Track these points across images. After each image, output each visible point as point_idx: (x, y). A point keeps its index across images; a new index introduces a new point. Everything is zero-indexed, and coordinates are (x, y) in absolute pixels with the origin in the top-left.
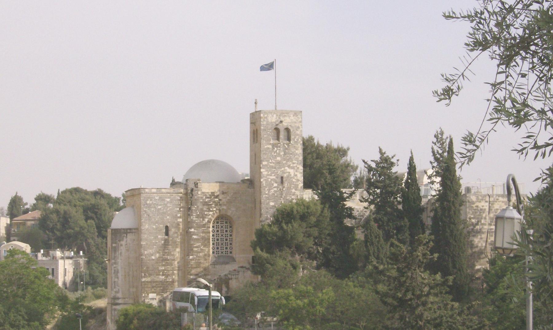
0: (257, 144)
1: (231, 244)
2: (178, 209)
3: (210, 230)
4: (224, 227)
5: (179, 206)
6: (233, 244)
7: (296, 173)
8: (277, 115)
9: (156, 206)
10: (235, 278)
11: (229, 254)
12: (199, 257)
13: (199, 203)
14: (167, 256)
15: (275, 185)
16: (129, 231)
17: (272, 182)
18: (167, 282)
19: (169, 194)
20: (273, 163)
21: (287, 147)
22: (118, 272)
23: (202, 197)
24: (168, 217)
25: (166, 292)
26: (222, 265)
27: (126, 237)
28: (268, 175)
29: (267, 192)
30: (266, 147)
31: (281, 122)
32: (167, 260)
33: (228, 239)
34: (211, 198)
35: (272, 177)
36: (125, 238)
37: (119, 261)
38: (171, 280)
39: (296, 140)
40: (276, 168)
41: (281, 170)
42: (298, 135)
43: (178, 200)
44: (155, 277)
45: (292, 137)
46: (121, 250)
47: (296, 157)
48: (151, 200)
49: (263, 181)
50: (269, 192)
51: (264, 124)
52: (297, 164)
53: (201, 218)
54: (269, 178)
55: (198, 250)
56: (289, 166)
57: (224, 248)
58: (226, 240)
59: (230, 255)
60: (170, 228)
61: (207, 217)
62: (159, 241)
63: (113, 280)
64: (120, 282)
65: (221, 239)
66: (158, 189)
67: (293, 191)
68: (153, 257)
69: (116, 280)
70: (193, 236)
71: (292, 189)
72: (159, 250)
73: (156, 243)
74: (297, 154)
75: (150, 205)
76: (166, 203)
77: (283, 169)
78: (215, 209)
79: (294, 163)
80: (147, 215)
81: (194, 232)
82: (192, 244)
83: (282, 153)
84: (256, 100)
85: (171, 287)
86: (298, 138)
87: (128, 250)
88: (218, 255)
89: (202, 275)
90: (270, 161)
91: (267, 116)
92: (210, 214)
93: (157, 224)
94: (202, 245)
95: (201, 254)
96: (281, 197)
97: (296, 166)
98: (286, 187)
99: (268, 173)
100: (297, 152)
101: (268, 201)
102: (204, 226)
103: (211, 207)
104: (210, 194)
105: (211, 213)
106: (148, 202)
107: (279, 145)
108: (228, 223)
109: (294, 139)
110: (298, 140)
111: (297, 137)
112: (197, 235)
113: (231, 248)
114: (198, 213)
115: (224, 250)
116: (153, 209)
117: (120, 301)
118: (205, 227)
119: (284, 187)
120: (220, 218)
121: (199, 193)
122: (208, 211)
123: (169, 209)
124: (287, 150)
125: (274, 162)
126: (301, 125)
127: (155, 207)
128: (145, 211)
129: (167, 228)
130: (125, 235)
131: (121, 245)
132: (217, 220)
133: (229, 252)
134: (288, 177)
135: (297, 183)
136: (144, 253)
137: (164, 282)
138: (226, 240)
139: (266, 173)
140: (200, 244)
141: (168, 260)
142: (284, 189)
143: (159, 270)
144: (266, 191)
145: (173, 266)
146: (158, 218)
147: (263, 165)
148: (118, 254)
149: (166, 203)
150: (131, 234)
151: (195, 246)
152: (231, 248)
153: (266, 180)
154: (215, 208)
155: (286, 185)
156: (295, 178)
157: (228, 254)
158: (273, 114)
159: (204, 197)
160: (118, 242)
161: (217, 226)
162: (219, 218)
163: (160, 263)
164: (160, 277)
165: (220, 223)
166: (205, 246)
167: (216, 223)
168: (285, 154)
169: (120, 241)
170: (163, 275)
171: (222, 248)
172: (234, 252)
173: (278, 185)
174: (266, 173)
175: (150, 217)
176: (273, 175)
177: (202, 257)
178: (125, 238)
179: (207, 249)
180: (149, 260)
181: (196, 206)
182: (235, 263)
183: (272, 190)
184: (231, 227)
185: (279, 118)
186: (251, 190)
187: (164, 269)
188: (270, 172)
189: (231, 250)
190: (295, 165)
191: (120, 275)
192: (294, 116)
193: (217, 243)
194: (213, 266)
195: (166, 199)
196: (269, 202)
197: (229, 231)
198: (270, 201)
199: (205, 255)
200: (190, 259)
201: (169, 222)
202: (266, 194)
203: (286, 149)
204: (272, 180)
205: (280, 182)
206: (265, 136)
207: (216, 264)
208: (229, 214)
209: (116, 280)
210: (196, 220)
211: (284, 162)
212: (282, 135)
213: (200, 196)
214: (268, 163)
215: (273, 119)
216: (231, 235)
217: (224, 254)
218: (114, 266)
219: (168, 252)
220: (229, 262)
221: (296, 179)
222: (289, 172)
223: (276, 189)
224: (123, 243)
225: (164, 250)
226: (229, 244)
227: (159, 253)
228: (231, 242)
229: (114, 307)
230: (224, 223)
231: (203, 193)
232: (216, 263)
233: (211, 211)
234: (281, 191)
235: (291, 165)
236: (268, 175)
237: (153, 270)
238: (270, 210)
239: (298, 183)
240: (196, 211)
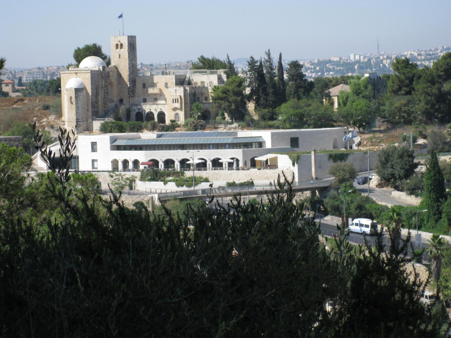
0: (122, 50)
22: (79, 107)
37: (79, 102)
64: (80, 112)
69: (78, 111)
117: (80, 120)
131: (80, 95)
148: (78, 99)
191: (80, 108)
209: (78, 111)
212: (132, 47)
224: (81, 94)
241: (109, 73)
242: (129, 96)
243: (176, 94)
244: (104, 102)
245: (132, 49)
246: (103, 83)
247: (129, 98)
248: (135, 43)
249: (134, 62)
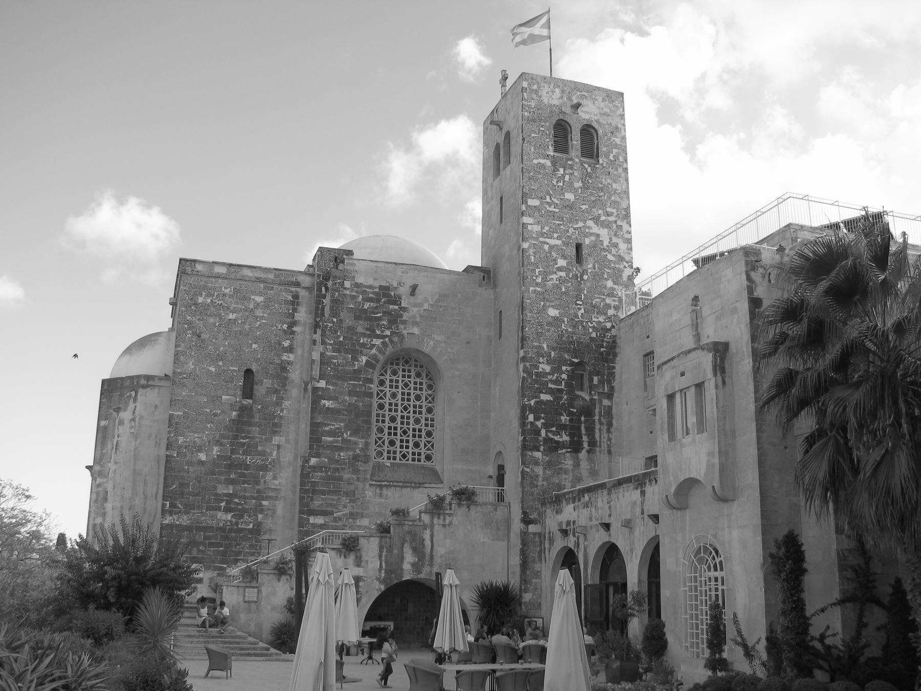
1: (429, 434)
2: (285, 327)
3: (371, 388)
4: (412, 385)
5: (289, 320)
6: (434, 434)
7: (615, 240)
8: (563, 91)
9: (222, 311)
10: (444, 526)
11: (422, 462)
12: (337, 462)
13: (345, 311)
14: (243, 454)
15: (562, 263)
16: (143, 382)
17: (554, 255)
18: (240, 531)
19: (262, 286)
20: (556, 206)
21: (589, 170)
22: (105, 499)
23: (354, 297)
24: (254, 346)
25: (236, 561)
26: (404, 490)
27: (135, 400)
28: (542, 234)
29: (539, 280)
30: (535, 161)
31: (577, 106)
32: (244, 466)
33: (423, 421)
34: (378, 301)
35: (552, 242)
36: (132, 400)
37: (111, 466)
38: (251, 526)
39: (611, 158)
40: (563, 220)
41: (575, 226)
42: (616, 146)
43: (286, 302)
44: (203, 514)
45: (604, 149)
46: (118, 436)
47: (613, 198)
48: (209, 295)
49: (530, 247)
50: (545, 279)
51: (529, 106)
52: (617, 216)
53: (347, 351)
55: (337, 441)
56: (596, 220)
57: (411, 444)
58: (417, 421)
59: (428, 463)
60: (257, 377)
61: (365, 351)
62: (223, 412)
63: (91, 519)
65: (402, 417)
66: (231, 265)
67: (610, 284)
68: (203, 457)
70: (323, 402)
71: (606, 279)
72: (222, 436)
73: (215, 415)
74: (615, 193)
75: (206, 306)
76: (251, 306)
77: (581, 224)
78: (388, 333)
79: (609, 214)
80: (194, 334)
81: (326, 388)
82: (319, 423)
83: (578, 184)
85: (252, 546)
86: (618, 154)
87: (135, 436)
88: (392, 461)
89: (344, 515)
90: (548, 200)
91: (539, 88)
92: (374, 345)
93: (221, 363)
94: (347, 427)
95: (342, 454)
96: (578, 297)
97: (616, 222)
98: (589, 271)
99: (542, 228)
100: (614, 186)
101: (542, 303)
102: (356, 375)
103: (378, 325)
104: (377, 290)
105: (377, 342)
106: (200, 300)
107: (570, 162)
108: (424, 375)
109: (607, 156)
110: (616, 157)
111: (615, 151)
112: (335, 399)
113: (429, 446)
114: (341, 339)
115: (410, 450)
116: (212, 320)
118: (359, 379)
119: (584, 272)
120: (401, 362)
121: (347, 284)
122: (369, 336)
123: (258, 323)
124: (591, 177)
125: (558, 202)
126: (624, 125)
127: (220, 315)
128: (190, 323)
129: (248, 373)
130: (133, 393)
131: (121, 422)
132: (392, 364)
133: (423, 457)
134: (594, 246)
135: (617, 266)
136: (177, 440)
137: (231, 530)
138: (417, 421)
139: (537, 228)
140: (342, 424)
141: (247, 467)
142: (585, 277)
143: (220, 495)
144: (536, 277)
145: (261, 487)
146: (225, 346)
147: (528, 206)
148: (109, 446)
149: (251, 306)
150: (148, 389)
151: (327, 429)
152: (429, 446)
153: (538, 248)
154: (388, 329)
155: (590, 266)
156: (614, 251)
157: (419, 460)
158: (552, 85)
159: (361, 297)
160: (115, 414)
161: (391, 381)
162: (398, 359)
163: (221, 473)
164: (220, 515)
165: (401, 373)
166: (355, 433)
167: (389, 372)
168: (585, 187)
169: (118, 410)
170: (227, 510)
171: (405, 444)
172: (436, 454)
173: (568, 263)
174: (537, 228)
175: (203, 341)
176: (555, 235)
177: (345, 464)
178: (132, 400)
179: (361, 443)
180: (190, 464)
181: (335, 320)
182: (440, 486)
183: (554, 276)
184: (430, 387)
185: (570, 99)
186: (486, 293)
187: (231, 492)
188: (547, 228)
189: (428, 449)
190: (612, 219)
191: (109, 506)
192: (603, 100)
193: (390, 428)
194: (378, 491)
195: (253, 297)
196: (544, 305)
197: (427, 399)
198: (548, 304)
199: (356, 458)
200: (310, 467)
201: (257, 360)
202: (537, 284)
203: (589, 175)
204: (552, 247)
205: (574, 257)
206: (533, 135)
207: (385, 486)
208: (427, 350)
210: (333, 357)
211: (584, 207)
212: (576, 141)
213: (348, 292)
214: (542, 203)
215: (553, 98)
216: (430, 411)
217: (410, 462)
219: (249, 444)
220: (424, 484)
221: (614, 255)
222: (598, 235)
223: (563, 274)
224: (126, 415)
225: (236, 437)
226: (423, 434)
227: (221, 445)
228: (429, 428)
230: (413, 374)
231: (357, 285)
232: (385, 483)
233: (378, 337)
234: (579, 279)
235: (603, 218)
236: (542, 234)
237: (198, 494)
238: (549, 331)
239: (622, 267)
240: (336, 332)
241: (396, 300)
243: (698, 337)
244: (305, 476)
246: (316, 356)
247: (523, 455)
248: (618, 130)
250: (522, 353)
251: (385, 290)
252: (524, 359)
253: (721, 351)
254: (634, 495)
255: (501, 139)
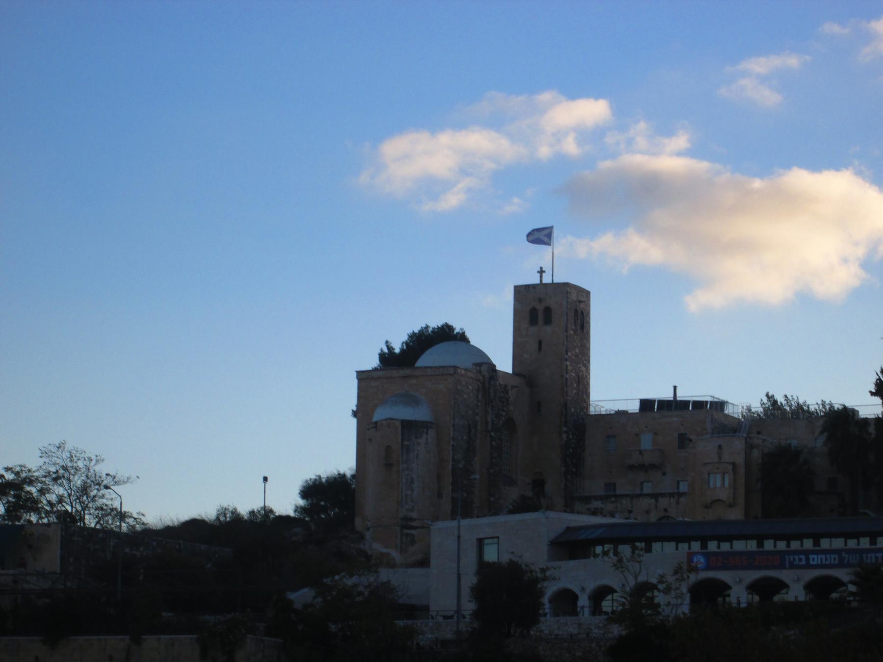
0: (548, 329)
22: (412, 482)
27: (427, 433)
54: (571, 375)
56: (583, 363)
69: (409, 492)
84: (541, 268)
130: (425, 430)
131: (419, 444)
209: (409, 492)
218: (407, 472)
222: (583, 371)
229: (406, 531)
231: (500, 384)
242: (563, 469)
243: (720, 457)
245: (579, 327)
249: (583, 369)
250: (565, 429)
251: (506, 386)
252: (566, 432)
253: (734, 464)
254: (653, 501)
255: (540, 308)
